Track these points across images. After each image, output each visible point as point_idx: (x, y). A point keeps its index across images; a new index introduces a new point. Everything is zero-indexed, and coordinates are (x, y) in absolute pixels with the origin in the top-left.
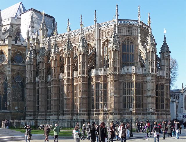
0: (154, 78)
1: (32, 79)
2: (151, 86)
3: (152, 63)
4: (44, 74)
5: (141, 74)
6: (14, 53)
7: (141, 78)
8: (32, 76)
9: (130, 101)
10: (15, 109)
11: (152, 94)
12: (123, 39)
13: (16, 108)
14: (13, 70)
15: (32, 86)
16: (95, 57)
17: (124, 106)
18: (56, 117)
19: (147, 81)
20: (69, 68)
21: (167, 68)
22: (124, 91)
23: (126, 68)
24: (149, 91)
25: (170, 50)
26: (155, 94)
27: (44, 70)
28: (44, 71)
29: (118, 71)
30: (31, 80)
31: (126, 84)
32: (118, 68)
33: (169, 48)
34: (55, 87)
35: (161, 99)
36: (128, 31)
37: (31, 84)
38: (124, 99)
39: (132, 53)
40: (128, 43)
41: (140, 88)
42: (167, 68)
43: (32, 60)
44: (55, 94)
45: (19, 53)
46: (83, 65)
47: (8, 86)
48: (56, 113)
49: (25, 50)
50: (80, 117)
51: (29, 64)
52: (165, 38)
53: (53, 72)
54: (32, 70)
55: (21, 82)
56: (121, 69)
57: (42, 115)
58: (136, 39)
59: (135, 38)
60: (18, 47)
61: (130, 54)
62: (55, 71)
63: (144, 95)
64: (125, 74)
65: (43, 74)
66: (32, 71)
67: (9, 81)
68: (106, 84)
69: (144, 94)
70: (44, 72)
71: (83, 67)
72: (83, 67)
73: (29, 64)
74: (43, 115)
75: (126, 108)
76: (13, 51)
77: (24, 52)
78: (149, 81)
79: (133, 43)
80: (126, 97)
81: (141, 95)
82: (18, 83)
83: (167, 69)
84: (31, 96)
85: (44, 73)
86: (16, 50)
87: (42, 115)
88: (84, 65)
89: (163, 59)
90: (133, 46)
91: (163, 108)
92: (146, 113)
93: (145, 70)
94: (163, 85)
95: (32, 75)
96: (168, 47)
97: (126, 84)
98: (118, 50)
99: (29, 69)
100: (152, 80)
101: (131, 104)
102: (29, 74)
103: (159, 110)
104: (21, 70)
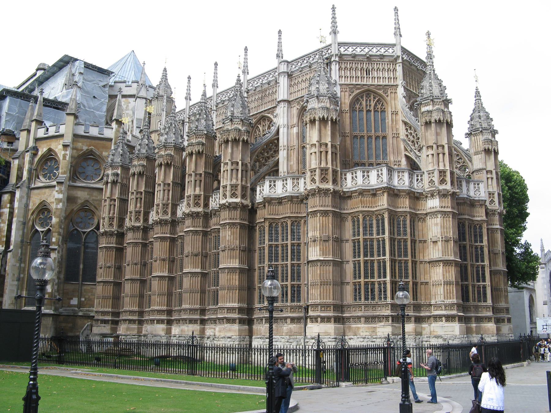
0: (448, 202)
1: (115, 223)
2: (443, 227)
3: (441, 156)
4: (143, 205)
5: (404, 191)
6: (79, 156)
7: (407, 202)
8: (114, 213)
9: (373, 277)
10: (71, 303)
11: (444, 252)
12: (354, 94)
13: (75, 301)
14: (70, 200)
15: (114, 239)
16: (277, 152)
17: (355, 296)
18: (163, 330)
19: (429, 211)
20: (198, 182)
21: (489, 176)
22: (354, 243)
23: (359, 174)
24: (435, 242)
25: (496, 125)
26: (455, 255)
27: (143, 195)
28: (141, 199)
29: (335, 181)
30: (111, 225)
31: (361, 220)
32: (335, 172)
33: (492, 120)
34: (162, 239)
35: (478, 271)
36: (368, 71)
37: (111, 234)
38: (355, 271)
39: (380, 133)
40: (370, 105)
41: (405, 234)
42: (489, 176)
43: (119, 172)
44: (164, 260)
45: (92, 155)
46: (234, 171)
47: (54, 240)
48: (164, 317)
49: (108, 148)
50: (220, 331)
51: (109, 181)
52: (478, 94)
53: (159, 198)
54: (117, 196)
55: (92, 230)
56: (345, 175)
57: (130, 321)
58: (393, 95)
59: (389, 92)
60: (89, 140)
61: (377, 137)
62: (166, 195)
63: (420, 257)
64: (355, 191)
65: (138, 205)
66: (115, 200)
67: (57, 227)
68: (299, 225)
69: (421, 255)
70: (143, 199)
71: (234, 176)
72: (234, 176)
73: (109, 181)
74: (135, 323)
75: (360, 299)
76: (75, 151)
77: (105, 154)
78: (434, 214)
79: (382, 105)
80: (359, 264)
81: (409, 258)
82: (84, 233)
83: (490, 180)
84: (109, 267)
85: (141, 204)
86: (85, 148)
87: (130, 321)
88: (238, 170)
89: (476, 153)
90: (383, 111)
91: (485, 301)
92: (429, 317)
93: (421, 180)
94: (481, 228)
95: (114, 210)
96: (488, 119)
97: (361, 220)
98: (332, 119)
99: (108, 194)
100: (443, 209)
101: (377, 286)
102: (107, 207)
103: (471, 303)
104: (93, 200)
